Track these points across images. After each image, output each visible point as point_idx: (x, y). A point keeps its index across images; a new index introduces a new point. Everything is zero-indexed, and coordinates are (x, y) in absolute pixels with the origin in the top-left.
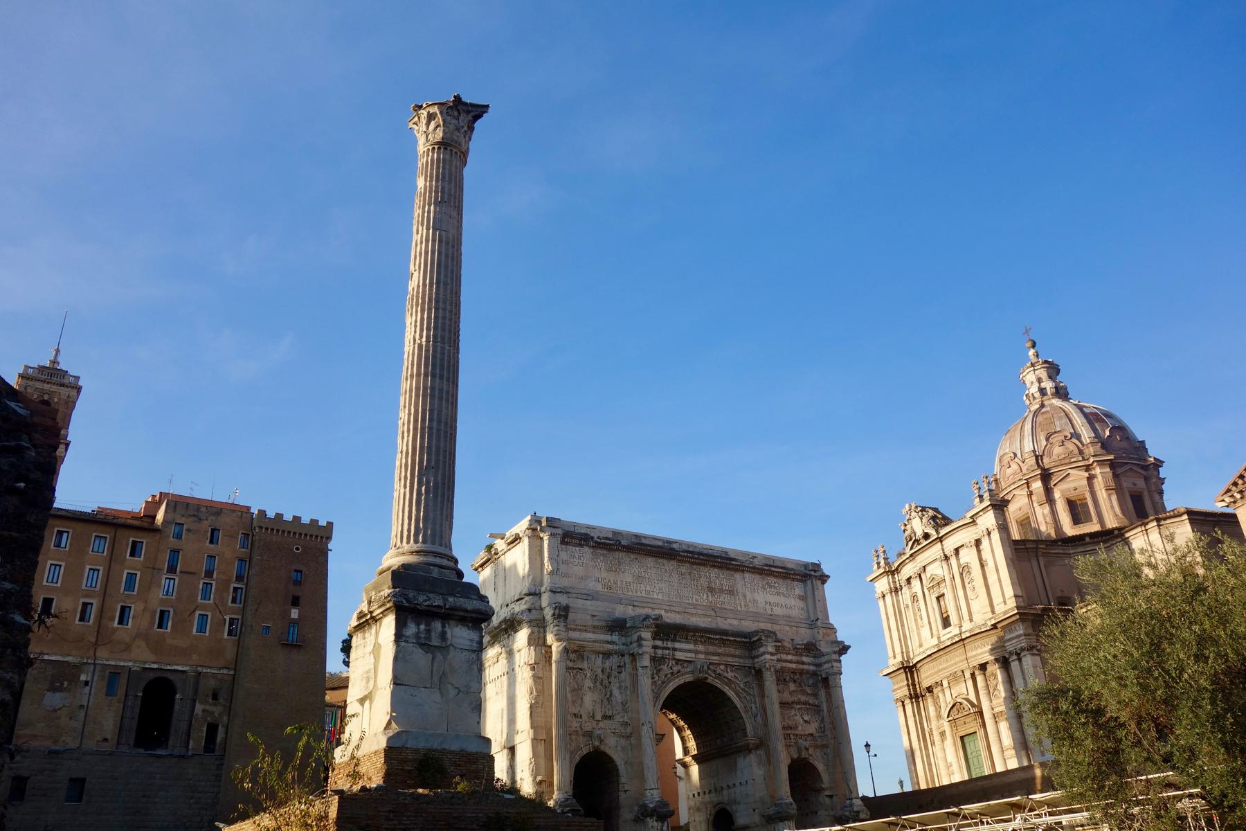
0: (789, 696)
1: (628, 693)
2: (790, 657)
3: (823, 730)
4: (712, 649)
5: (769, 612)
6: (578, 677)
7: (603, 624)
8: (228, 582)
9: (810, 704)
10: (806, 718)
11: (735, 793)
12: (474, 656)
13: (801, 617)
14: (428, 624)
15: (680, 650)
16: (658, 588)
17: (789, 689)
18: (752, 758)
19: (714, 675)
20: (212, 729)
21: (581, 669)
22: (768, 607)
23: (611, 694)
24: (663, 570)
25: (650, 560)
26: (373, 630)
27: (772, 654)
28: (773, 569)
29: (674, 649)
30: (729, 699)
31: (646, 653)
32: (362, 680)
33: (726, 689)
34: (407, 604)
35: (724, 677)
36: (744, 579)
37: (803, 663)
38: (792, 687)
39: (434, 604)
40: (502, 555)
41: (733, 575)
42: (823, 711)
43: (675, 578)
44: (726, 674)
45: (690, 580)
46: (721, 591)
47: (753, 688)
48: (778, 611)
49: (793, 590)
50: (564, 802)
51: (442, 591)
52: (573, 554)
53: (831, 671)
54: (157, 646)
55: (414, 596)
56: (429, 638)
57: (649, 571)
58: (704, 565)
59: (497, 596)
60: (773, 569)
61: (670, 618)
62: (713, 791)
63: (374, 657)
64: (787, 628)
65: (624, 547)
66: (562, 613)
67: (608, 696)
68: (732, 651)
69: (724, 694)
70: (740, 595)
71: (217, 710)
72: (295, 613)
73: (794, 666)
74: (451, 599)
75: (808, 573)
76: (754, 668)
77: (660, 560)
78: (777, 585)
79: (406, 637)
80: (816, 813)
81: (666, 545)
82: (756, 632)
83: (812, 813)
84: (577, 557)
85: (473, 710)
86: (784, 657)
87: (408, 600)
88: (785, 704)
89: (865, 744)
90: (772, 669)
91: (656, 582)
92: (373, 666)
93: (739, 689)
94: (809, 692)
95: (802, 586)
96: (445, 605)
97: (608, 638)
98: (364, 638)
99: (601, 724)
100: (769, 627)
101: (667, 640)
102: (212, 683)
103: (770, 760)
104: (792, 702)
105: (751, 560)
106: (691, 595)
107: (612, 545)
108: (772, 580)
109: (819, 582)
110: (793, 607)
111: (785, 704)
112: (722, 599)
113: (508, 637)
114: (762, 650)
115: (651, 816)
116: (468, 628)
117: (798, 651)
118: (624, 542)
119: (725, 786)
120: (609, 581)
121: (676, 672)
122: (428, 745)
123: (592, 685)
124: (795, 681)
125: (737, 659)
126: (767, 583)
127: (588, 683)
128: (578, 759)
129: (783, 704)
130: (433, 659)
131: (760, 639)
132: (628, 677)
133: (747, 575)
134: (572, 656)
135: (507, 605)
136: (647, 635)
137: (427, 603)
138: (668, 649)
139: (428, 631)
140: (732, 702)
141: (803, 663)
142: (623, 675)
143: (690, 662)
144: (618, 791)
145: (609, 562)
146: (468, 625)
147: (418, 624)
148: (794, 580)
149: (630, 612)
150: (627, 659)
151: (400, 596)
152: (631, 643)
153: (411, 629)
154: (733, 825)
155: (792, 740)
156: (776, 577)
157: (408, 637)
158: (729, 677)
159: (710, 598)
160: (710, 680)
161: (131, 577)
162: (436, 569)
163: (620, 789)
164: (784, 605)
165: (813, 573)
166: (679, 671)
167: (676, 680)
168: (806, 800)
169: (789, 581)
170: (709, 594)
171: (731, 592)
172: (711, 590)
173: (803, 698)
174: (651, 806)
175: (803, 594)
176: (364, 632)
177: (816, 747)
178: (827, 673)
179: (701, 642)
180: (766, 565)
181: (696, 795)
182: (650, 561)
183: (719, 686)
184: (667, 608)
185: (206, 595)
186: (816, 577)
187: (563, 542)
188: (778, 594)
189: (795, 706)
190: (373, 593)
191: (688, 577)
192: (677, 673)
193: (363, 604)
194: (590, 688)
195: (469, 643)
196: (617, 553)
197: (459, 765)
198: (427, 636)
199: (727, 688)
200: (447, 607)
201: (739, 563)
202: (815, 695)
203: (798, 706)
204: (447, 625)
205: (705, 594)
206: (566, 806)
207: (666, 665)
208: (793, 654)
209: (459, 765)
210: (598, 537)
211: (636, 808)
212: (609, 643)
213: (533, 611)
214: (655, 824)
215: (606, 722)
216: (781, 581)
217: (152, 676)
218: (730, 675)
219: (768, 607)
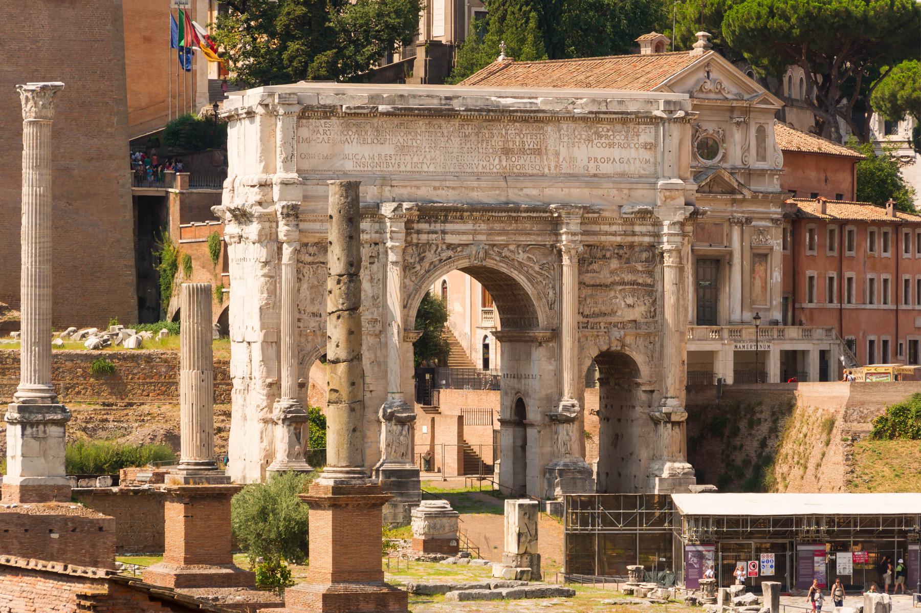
2: (614, 228)
3: (652, 314)
4: (497, 226)
5: (593, 171)
9: (638, 284)
10: (630, 301)
12: (61, 439)
14: (37, 427)
16: (428, 157)
17: (610, 267)
19: (498, 258)
21: (323, 263)
22: (592, 165)
24: (439, 134)
25: (421, 123)
29: (444, 232)
31: (397, 247)
33: (515, 274)
36: (559, 131)
37: (634, 234)
41: (542, 128)
42: (657, 290)
43: (456, 141)
46: (523, 151)
48: (606, 168)
49: (636, 138)
50: (287, 408)
56: (38, 434)
57: (419, 137)
58: (500, 121)
70: (550, 153)
73: (618, 239)
78: (611, 133)
84: (322, 132)
91: (427, 150)
94: (640, 268)
95: (653, 130)
101: (435, 222)
106: (476, 160)
108: (603, 128)
110: (632, 161)
112: (521, 162)
120: (363, 157)
121: (444, 258)
122: (39, 483)
125: (533, 237)
126: (595, 133)
141: (634, 234)
143: (467, 245)
145: (363, 133)
153: (29, 431)
156: (611, 121)
159: (504, 163)
164: (617, 160)
166: (450, 258)
170: (504, 157)
171: (537, 152)
172: (507, 152)
173: (629, 277)
179: (483, 221)
182: (421, 124)
183: (505, 270)
184: (437, 184)
188: (611, 145)
189: (615, 287)
191: (473, 138)
203: (621, 287)
207: (432, 252)
208: (619, 224)
216: (619, 127)
218: (522, 256)
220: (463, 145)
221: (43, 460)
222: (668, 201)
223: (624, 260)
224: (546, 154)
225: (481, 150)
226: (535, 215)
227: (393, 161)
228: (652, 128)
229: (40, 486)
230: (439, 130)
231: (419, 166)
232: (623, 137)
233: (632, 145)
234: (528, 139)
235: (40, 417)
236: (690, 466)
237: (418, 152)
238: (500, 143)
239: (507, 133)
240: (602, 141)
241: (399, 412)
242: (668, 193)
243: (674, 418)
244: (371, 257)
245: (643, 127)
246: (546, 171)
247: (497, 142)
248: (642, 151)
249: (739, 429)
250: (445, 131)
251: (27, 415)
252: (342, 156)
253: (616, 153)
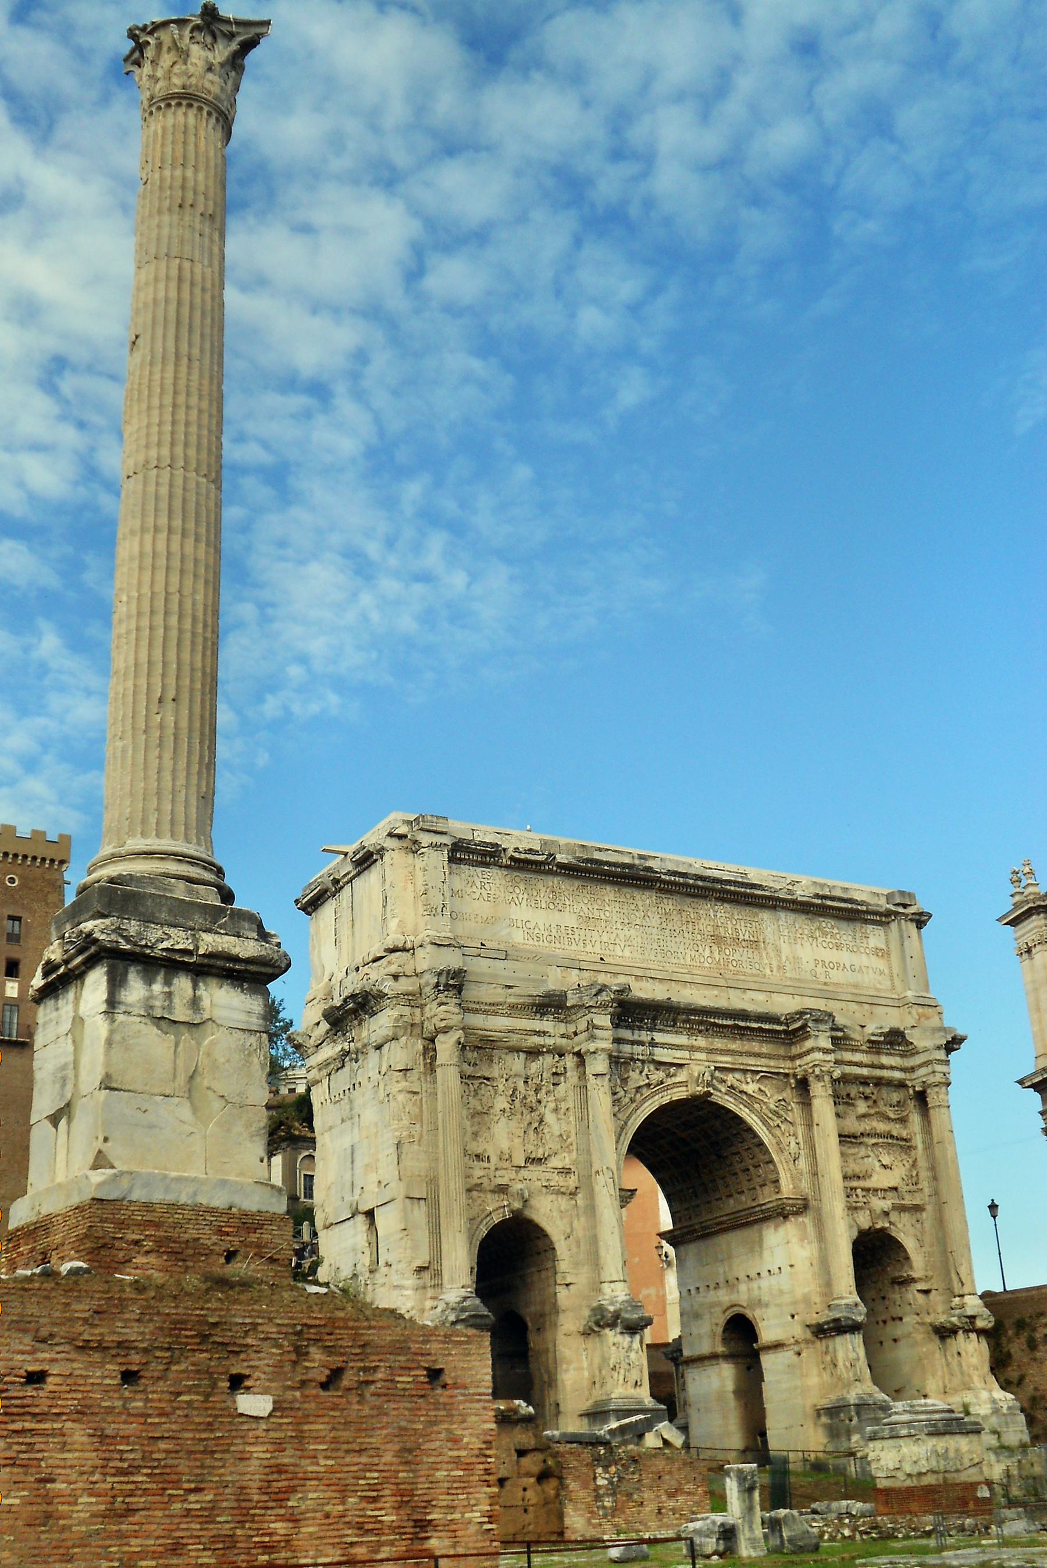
0: (856, 1124)
1: (572, 1119)
2: (858, 1057)
3: (914, 1180)
4: (719, 1043)
5: (822, 979)
6: (482, 1092)
7: (530, 1000)
9: (892, 1137)
10: (886, 1160)
11: (759, 1288)
12: (253, 1040)
13: (878, 986)
14: (168, 982)
15: (663, 1045)
16: (622, 937)
21: (488, 1079)
22: (820, 970)
23: (541, 1121)
26: (71, 995)
27: (826, 1051)
28: (829, 903)
29: (653, 1044)
30: (750, 1130)
31: (603, 1050)
32: (54, 1082)
33: (744, 1113)
34: (128, 947)
35: (741, 1092)
37: (882, 1067)
38: (862, 1107)
39: (177, 947)
40: (347, 883)
41: (757, 915)
42: (915, 1148)
43: (655, 920)
44: (744, 1087)
45: (679, 924)
47: (792, 1110)
48: (836, 976)
49: (865, 940)
50: (459, 1303)
51: (191, 923)
52: (470, 879)
53: (931, 1079)
55: (139, 933)
56: (170, 1008)
58: (705, 897)
59: (340, 952)
60: (829, 903)
61: (643, 991)
62: (721, 1285)
63: (74, 1041)
64: (854, 1006)
65: (561, 866)
66: (451, 982)
67: (536, 1125)
68: (756, 1047)
69: (738, 1120)
70: (770, 949)
73: (865, 1071)
74: (208, 938)
75: (893, 908)
76: (795, 1075)
77: (625, 890)
78: (835, 931)
79: (126, 1005)
80: (901, 1319)
81: (637, 862)
82: (801, 1013)
83: (893, 1319)
84: (478, 884)
85: (252, 1136)
86: (848, 1056)
87: (127, 939)
88: (849, 1137)
89: (990, 1203)
90: (827, 1078)
92: (71, 1058)
93: (767, 1112)
94: (892, 1116)
95: (882, 933)
96: (197, 948)
97: (537, 1025)
98: (57, 1009)
99: (524, 1173)
100: (820, 1005)
101: (640, 1028)
104: (862, 1134)
105: (790, 887)
107: (541, 863)
108: (827, 924)
109: (912, 927)
110: (864, 970)
111: (849, 1137)
112: (737, 956)
113: (360, 1024)
114: (809, 1044)
115: (612, 1325)
116: (242, 991)
117: (873, 1047)
118: (561, 858)
119: (742, 1276)
122: (170, 1198)
123: (507, 1106)
124: (867, 1098)
125: (763, 1061)
127: (502, 1102)
128: (484, 1231)
129: (846, 1138)
130: (177, 1045)
131: (804, 1027)
132: (571, 1093)
133: (782, 915)
134: (472, 1056)
135: (357, 969)
136: (604, 1020)
137: (165, 945)
138: (641, 1043)
139: (169, 995)
140: (755, 1135)
141: (882, 1067)
142: (562, 1088)
143: (681, 1066)
144: (556, 1284)
145: (535, 894)
146: (242, 986)
147: (149, 982)
148: (866, 921)
150: (570, 1061)
151: (114, 931)
152: (576, 1034)
153: (135, 990)
154: (756, 1341)
155: (861, 1199)
157: (131, 1005)
158: (750, 1092)
160: (718, 1098)
162: (182, 884)
163: (559, 1282)
165: (901, 910)
167: (656, 1097)
168: (884, 1298)
169: (858, 925)
170: (715, 948)
171: (754, 944)
172: (717, 939)
173: (882, 1127)
174: (611, 1308)
175: (884, 947)
176: (57, 998)
177: (902, 1209)
178: (924, 1082)
180: (817, 896)
181: (693, 1292)
182: (609, 893)
183: (731, 1107)
184: (640, 973)
186: (906, 915)
187: (452, 860)
188: (838, 947)
189: (866, 1140)
190: (68, 926)
191: (676, 918)
192: (658, 1085)
193: (52, 948)
194: (503, 1111)
195: (243, 1017)
196: (550, 878)
197: (227, 1234)
198: (166, 1004)
199: (747, 1110)
200: (201, 952)
201: (767, 893)
202: (903, 1121)
203: (874, 1141)
204: (201, 984)
205: (707, 948)
206: (463, 1310)
207: (638, 1071)
208: (863, 1051)
209: (227, 1234)
210: (516, 850)
211: (587, 1313)
212: (537, 1033)
213: (402, 980)
214: (619, 1338)
215: (531, 1168)
216: (843, 925)
218: (751, 1088)
219: (820, 970)
220: (664, 925)
221: (185, 1112)
222: (922, 1019)
223: (870, 1103)
224: (765, 949)
225: (686, 935)
226: (767, 1027)
227: (576, 937)
228: (879, 931)
229: (174, 1207)
230: (631, 901)
231: (611, 947)
232: (850, 938)
233: (862, 950)
234: (741, 927)
235: (179, 940)
236: (1013, 1397)
237: (608, 929)
238: (710, 928)
239: (715, 916)
240: (828, 940)
241: (627, 1311)
242: (920, 1010)
243: (980, 1324)
244: (554, 1074)
245: (870, 927)
246: (768, 971)
247: (705, 926)
248: (873, 958)
249: (1009, 1355)
250: (640, 904)
251: (133, 927)
252: (507, 922)
253: (845, 957)
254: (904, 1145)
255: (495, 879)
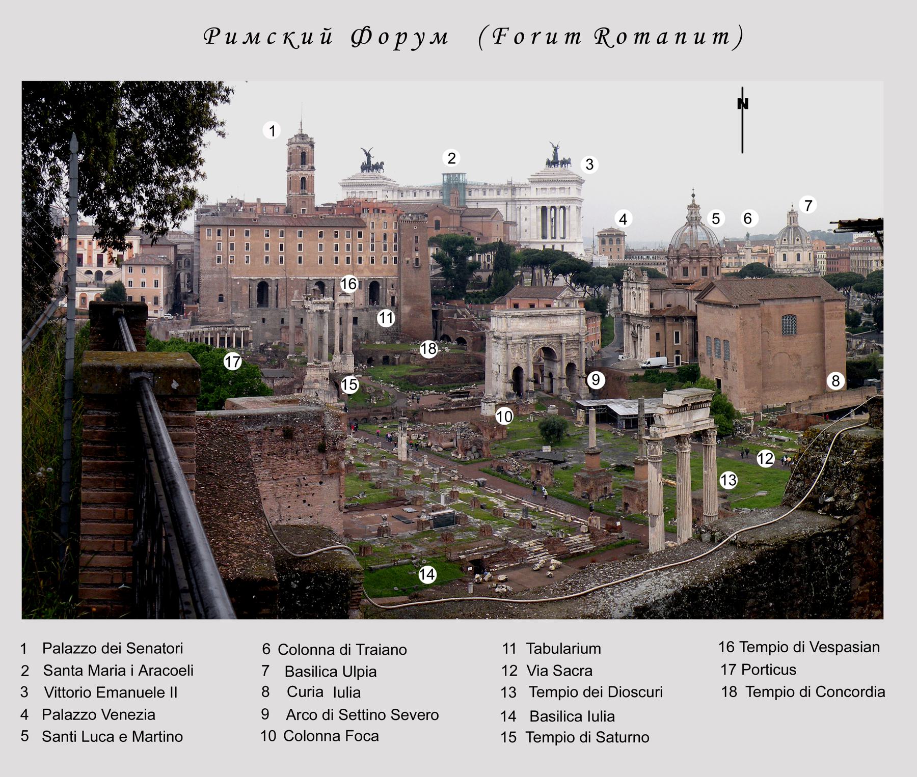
8: (392, 243)
18: (558, 364)
20: (393, 298)
54: (372, 270)
71: (394, 291)
72: (417, 254)
102: (391, 282)
103: (562, 364)
149: (528, 333)
161: (360, 245)
185: (385, 249)
217: (371, 281)
254: (578, 349)
255: (517, 319)
